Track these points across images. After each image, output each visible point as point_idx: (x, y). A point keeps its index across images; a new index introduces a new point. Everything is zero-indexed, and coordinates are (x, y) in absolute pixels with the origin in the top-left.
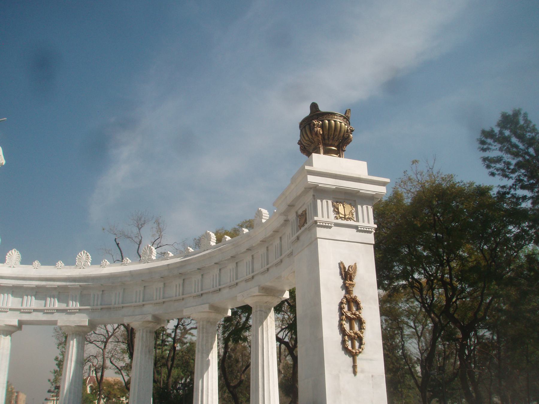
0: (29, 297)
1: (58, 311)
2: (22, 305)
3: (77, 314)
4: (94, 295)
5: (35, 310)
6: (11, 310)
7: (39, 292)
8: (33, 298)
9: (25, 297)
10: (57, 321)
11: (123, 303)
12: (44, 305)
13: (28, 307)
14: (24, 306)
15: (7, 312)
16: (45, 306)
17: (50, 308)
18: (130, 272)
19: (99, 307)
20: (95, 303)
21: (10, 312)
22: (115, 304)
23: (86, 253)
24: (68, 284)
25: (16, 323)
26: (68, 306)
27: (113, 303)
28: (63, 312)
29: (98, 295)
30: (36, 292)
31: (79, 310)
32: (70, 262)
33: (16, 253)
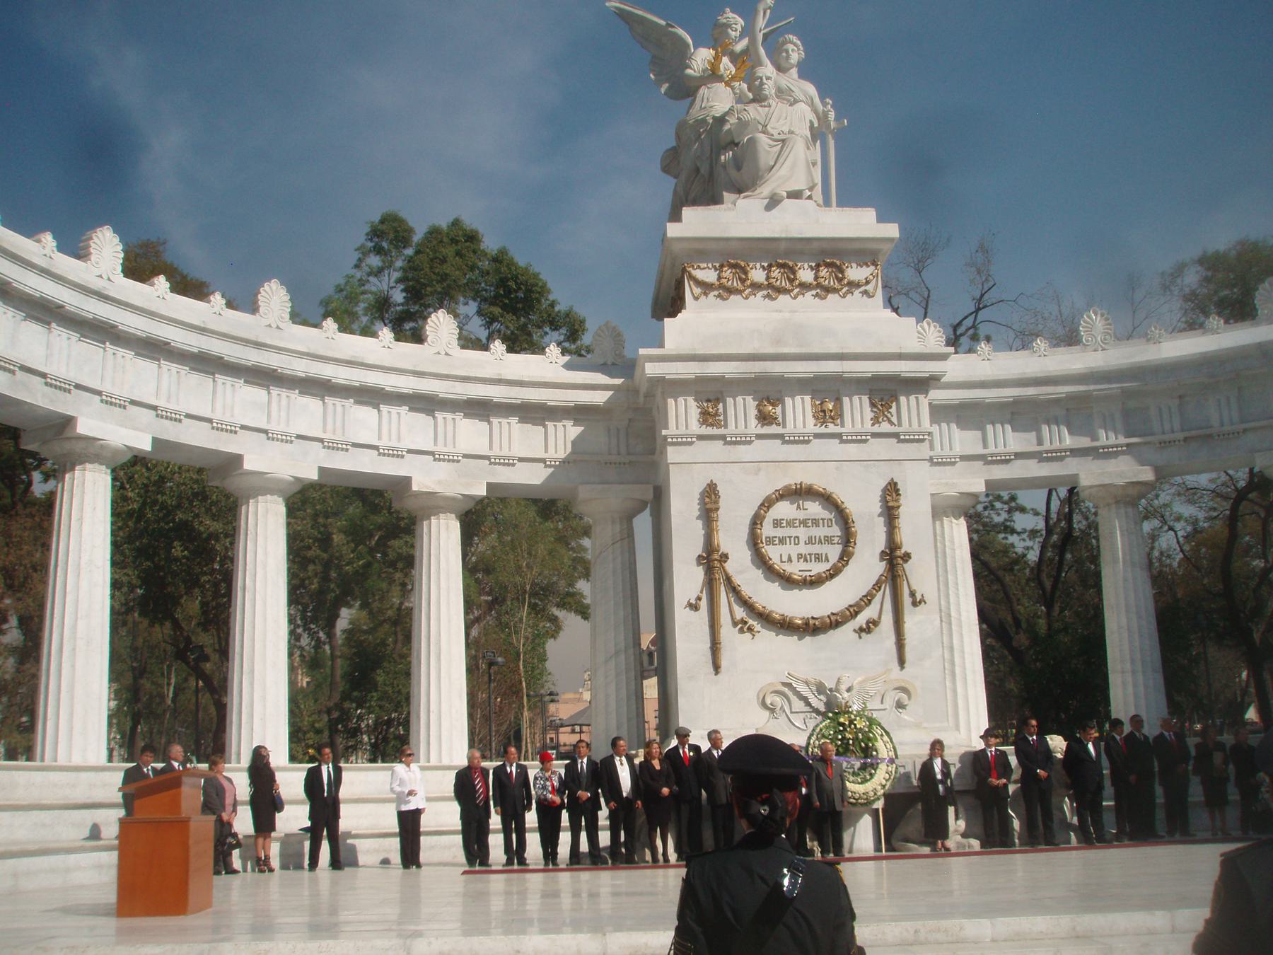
0: (999, 426)
1: (1075, 452)
2: (985, 446)
3: (1121, 458)
4: (1170, 409)
5: (1019, 456)
6: (964, 458)
7: (1021, 413)
8: (1008, 427)
9: (989, 428)
10: (1077, 475)
11: (1242, 422)
12: (1034, 441)
13: (1001, 449)
14: (992, 449)
15: (953, 464)
16: (1040, 443)
17: (1053, 447)
18: (1260, 346)
19: (1181, 436)
20: (1167, 427)
21: (960, 465)
22: (1222, 424)
23: (1102, 315)
24: (1092, 387)
25: (979, 487)
26: (1095, 438)
27: (1215, 421)
28: (1087, 455)
29: (1170, 409)
30: (1013, 413)
31: (1128, 445)
32: (1070, 338)
33: (932, 328)
